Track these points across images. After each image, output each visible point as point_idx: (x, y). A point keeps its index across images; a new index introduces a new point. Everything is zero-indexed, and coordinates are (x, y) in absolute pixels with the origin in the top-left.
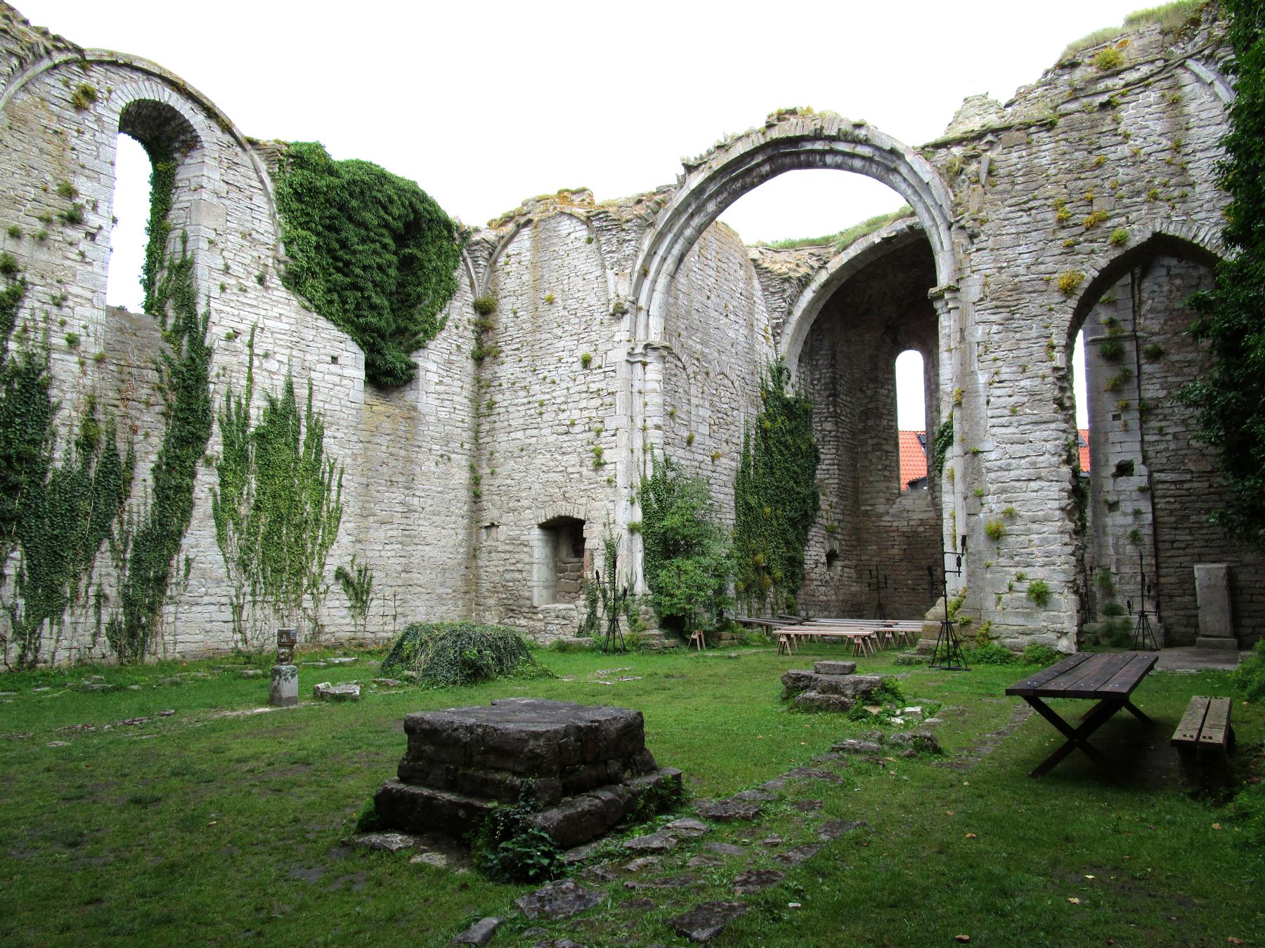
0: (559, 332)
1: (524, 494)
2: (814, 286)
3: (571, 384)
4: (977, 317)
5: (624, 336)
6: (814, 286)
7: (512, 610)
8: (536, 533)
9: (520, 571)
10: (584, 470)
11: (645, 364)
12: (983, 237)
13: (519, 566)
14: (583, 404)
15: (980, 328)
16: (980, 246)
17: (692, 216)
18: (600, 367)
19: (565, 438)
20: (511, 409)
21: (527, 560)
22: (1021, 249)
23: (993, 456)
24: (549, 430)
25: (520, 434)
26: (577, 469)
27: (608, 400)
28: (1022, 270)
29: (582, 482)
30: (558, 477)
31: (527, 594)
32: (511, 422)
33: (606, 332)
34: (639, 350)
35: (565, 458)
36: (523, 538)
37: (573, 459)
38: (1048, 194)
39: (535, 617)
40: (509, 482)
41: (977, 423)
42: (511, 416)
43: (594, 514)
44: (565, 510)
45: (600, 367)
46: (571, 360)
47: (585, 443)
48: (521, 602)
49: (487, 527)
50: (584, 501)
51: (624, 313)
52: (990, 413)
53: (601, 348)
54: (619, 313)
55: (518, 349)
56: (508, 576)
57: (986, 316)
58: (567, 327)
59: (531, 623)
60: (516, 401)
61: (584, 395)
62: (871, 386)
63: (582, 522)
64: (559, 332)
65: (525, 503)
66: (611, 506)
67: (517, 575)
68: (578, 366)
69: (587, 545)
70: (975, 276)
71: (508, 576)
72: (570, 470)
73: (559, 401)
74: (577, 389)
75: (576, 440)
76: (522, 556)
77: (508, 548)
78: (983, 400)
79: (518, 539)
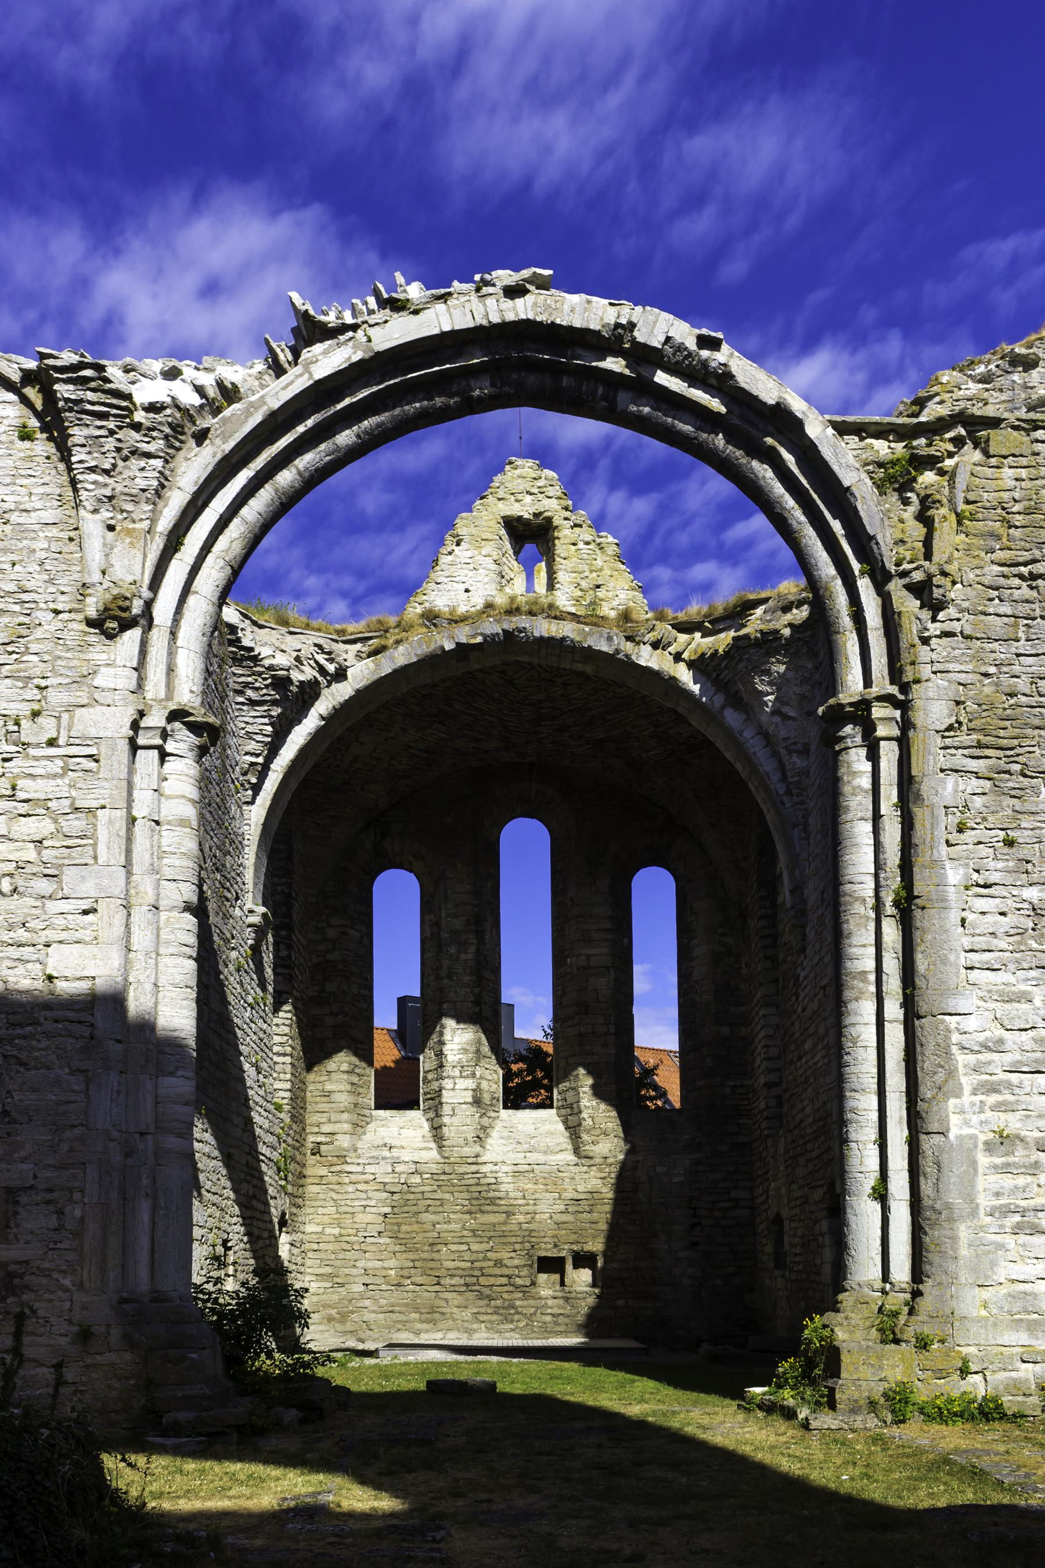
2: (323, 706)
4: (942, 761)
5: (127, 680)
6: (323, 706)
11: (163, 756)
12: (952, 611)
15: (951, 780)
16: (948, 626)
18: (52, 743)
22: (1023, 646)
23: (970, 1024)
28: (1022, 684)
33: (72, 662)
34: (156, 719)
41: (944, 961)
45: (52, 743)
51: (126, 625)
52: (967, 942)
53: (56, 698)
54: (115, 619)
57: (959, 760)
62: (335, 921)
70: (939, 681)
78: (954, 916)
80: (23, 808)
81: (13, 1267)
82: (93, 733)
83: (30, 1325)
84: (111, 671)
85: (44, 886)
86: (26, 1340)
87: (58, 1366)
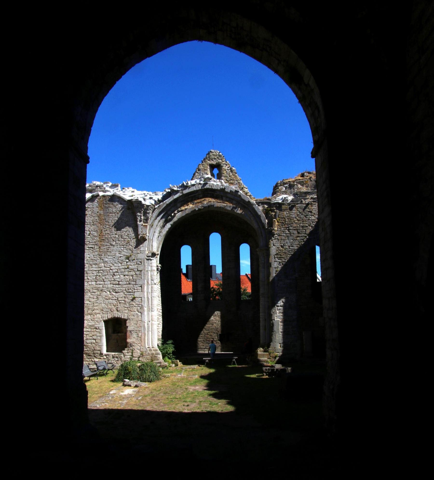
0: (114, 243)
1: (96, 308)
3: (120, 265)
7: (89, 356)
8: (103, 324)
9: (95, 340)
10: (127, 300)
14: (126, 273)
19: (117, 286)
21: (98, 334)
24: (109, 282)
29: (125, 304)
30: (114, 302)
31: (98, 349)
32: (89, 278)
35: (117, 294)
36: (96, 326)
37: (122, 294)
38: (294, 226)
39: (102, 358)
42: (89, 275)
43: (131, 317)
46: (120, 255)
47: (127, 289)
48: (96, 352)
50: (126, 311)
55: (92, 248)
58: (117, 242)
59: (100, 360)
60: (92, 269)
61: (126, 270)
63: (125, 320)
65: (97, 311)
66: (139, 314)
67: (94, 341)
68: (123, 258)
69: (129, 329)
73: (114, 271)
74: (123, 267)
75: (122, 287)
76: (96, 333)
79: (93, 326)
80: (130, 270)
83: (134, 351)
85: (134, 283)
86: (134, 354)
87: (139, 358)
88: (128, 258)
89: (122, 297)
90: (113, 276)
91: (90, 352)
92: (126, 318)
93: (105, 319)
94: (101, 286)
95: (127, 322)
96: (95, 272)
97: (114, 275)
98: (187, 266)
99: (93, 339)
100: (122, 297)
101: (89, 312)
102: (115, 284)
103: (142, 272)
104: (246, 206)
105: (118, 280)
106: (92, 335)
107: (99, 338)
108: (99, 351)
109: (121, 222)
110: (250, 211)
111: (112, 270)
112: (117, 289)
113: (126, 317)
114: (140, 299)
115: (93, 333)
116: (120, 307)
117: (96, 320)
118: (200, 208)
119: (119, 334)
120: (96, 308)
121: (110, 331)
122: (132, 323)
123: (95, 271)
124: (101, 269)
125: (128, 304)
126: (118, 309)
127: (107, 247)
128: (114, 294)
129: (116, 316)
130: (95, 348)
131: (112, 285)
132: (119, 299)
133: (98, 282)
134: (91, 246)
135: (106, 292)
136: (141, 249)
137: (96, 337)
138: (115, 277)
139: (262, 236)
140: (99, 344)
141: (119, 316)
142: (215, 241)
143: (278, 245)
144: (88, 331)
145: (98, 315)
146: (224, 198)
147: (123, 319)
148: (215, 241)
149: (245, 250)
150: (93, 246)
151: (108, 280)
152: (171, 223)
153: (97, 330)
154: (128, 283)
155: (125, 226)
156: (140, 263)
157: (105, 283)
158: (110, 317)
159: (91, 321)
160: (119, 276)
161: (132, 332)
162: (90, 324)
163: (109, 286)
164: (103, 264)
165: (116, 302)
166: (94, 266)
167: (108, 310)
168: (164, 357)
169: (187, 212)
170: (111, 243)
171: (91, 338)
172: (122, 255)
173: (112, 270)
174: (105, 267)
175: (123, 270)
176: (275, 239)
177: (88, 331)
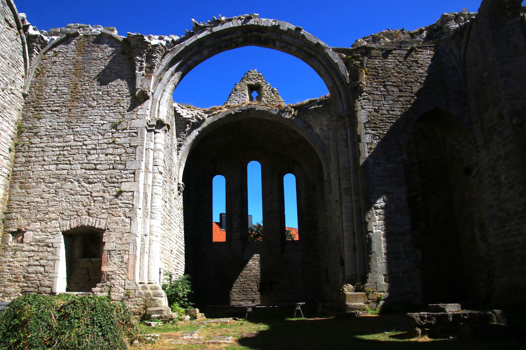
0: (94, 104)
1: (51, 209)
3: (100, 137)
8: (61, 239)
9: (44, 266)
10: (107, 195)
13: (43, 262)
14: (110, 151)
17: (193, 55)
19: (92, 172)
20: (46, 149)
21: (50, 257)
25: (53, 167)
26: (101, 194)
27: (130, 150)
29: (104, 203)
30: (84, 198)
31: (47, 283)
32: (46, 158)
35: (91, 186)
37: (99, 186)
38: (393, 81)
40: (39, 200)
43: (112, 226)
44: (88, 221)
46: (102, 122)
48: (42, 289)
49: (13, 233)
50: (104, 216)
56: (30, 269)
58: (100, 101)
60: (52, 144)
61: (110, 145)
63: (101, 232)
64: (94, 104)
65: (53, 216)
66: (128, 220)
67: (42, 269)
68: (107, 127)
69: (107, 247)
71: (30, 269)
72: (94, 194)
73: (89, 147)
74: (105, 141)
76: (46, 254)
77: (32, 248)
79: (43, 241)
80: (117, 146)
81: (109, 273)
82: (136, 126)
83: (113, 289)
84: (142, 110)
86: (112, 293)
87: (122, 301)
88: (115, 126)
89: (98, 191)
90: (87, 156)
91: (32, 289)
92: (103, 228)
93: (65, 229)
94: (65, 172)
95: (104, 234)
96: (57, 149)
97: (89, 153)
98: (221, 215)
99: (41, 265)
100: (98, 191)
101: (39, 216)
102: (90, 169)
103: (138, 149)
104: (313, 53)
105: (95, 162)
106: (38, 258)
107: (51, 263)
108: (49, 287)
109: (110, 72)
110: (320, 62)
111: (86, 145)
112: (91, 177)
113: (102, 226)
114: (130, 194)
115: (41, 254)
116: (95, 208)
117: (49, 230)
118: (237, 111)
119: (93, 259)
120: (51, 209)
121: (77, 252)
122: (114, 236)
123: (58, 147)
124: (69, 144)
125: (108, 203)
126: (90, 212)
127: (83, 109)
128: (86, 185)
129: (86, 224)
130: (42, 282)
131: (84, 170)
132: (94, 194)
133: (61, 166)
134: (56, 108)
135: (72, 182)
136: (138, 113)
137: (45, 261)
138: (90, 157)
139: (341, 97)
140: (50, 275)
141: (90, 225)
142: (254, 171)
143: (369, 107)
144: (33, 251)
145: (55, 221)
146: (277, 44)
147: (98, 229)
148: (254, 171)
149: (290, 182)
150: (59, 108)
151: (77, 162)
152: (199, 129)
153: (49, 249)
154: (111, 167)
155: (116, 78)
156: (134, 134)
157: (72, 167)
158: (74, 224)
159: (40, 233)
160: (97, 156)
161: (113, 254)
162: (37, 237)
163: (79, 172)
164: (72, 136)
165: (87, 200)
166: (56, 139)
167: (72, 213)
168: (171, 302)
169: (220, 116)
170: (90, 103)
171: (36, 263)
172: (105, 122)
173: (86, 145)
174: (75, 140)
175: (105, 146)
176: (364, 99)
177: (33, 251)
